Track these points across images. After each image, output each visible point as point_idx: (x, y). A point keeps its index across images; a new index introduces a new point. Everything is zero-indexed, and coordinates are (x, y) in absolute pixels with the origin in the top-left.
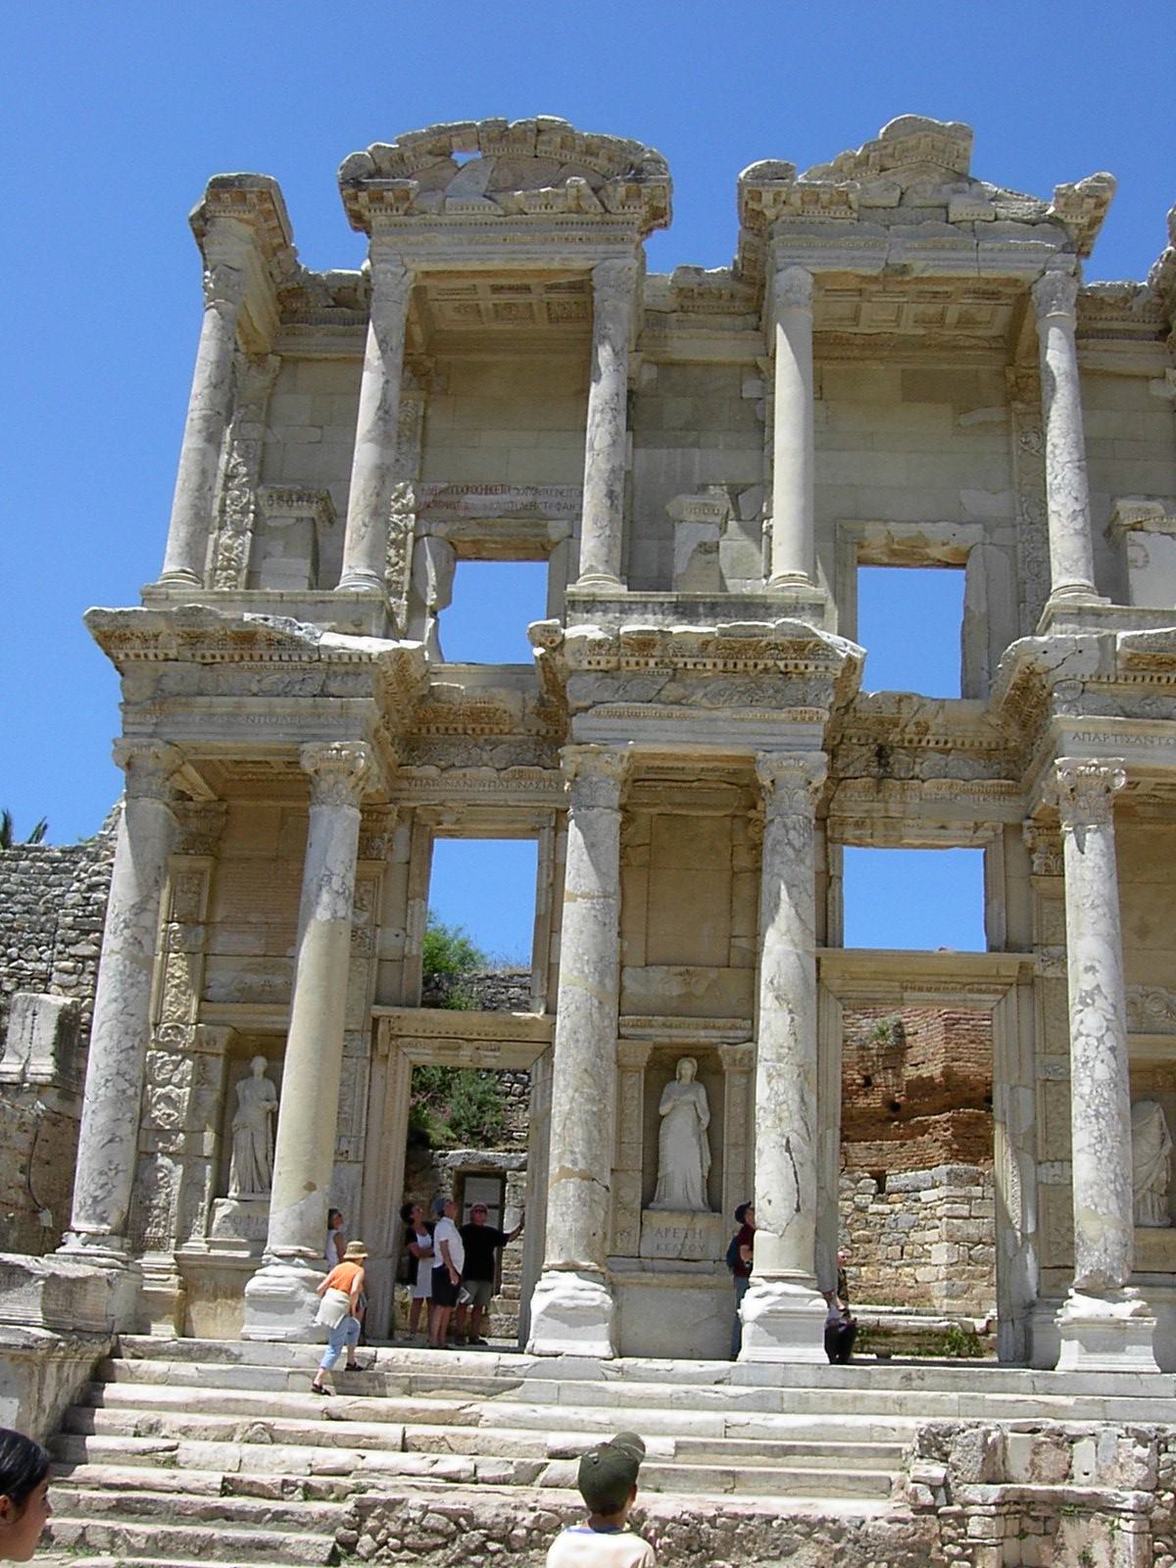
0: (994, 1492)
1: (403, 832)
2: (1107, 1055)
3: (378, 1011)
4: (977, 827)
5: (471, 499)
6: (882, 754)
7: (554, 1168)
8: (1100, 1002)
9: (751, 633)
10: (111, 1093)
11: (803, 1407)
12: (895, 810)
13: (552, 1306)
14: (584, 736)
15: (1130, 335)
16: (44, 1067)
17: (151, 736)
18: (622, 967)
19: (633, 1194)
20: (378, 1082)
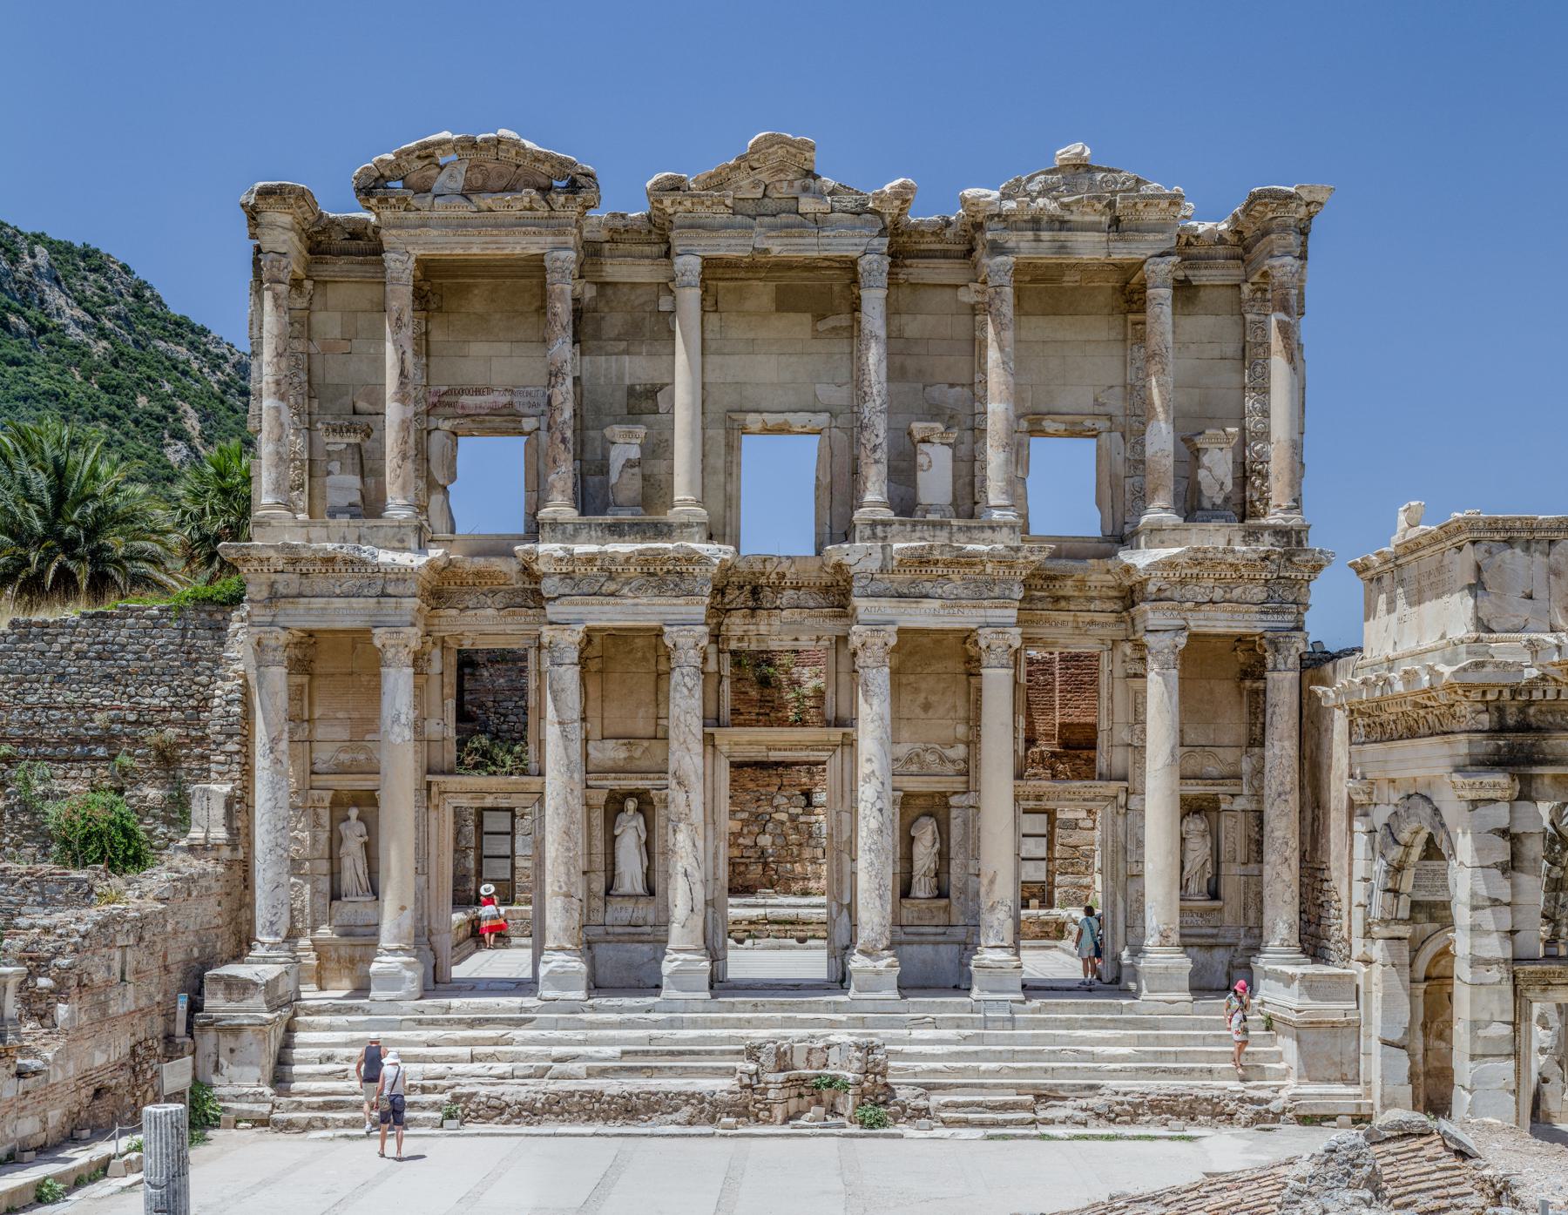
0: (781, 1076)
1: (437, 652)
2: (877, 814)
3: (429, 778)
4: (818, 639)
5: (466, 400)
6: (755, 591)
7: (548, 890)
8: (874, 780)
9: (657, 556)
10: (274, 858)
11: (694, 1024)
12: (763, 629)
13: (551, 971)
14: (553, 618)
15: (945, 255)
16: (220, 834)
17: (271, 624)
18: (587, 740)
19: (599, 885)
20: (433, 822)
